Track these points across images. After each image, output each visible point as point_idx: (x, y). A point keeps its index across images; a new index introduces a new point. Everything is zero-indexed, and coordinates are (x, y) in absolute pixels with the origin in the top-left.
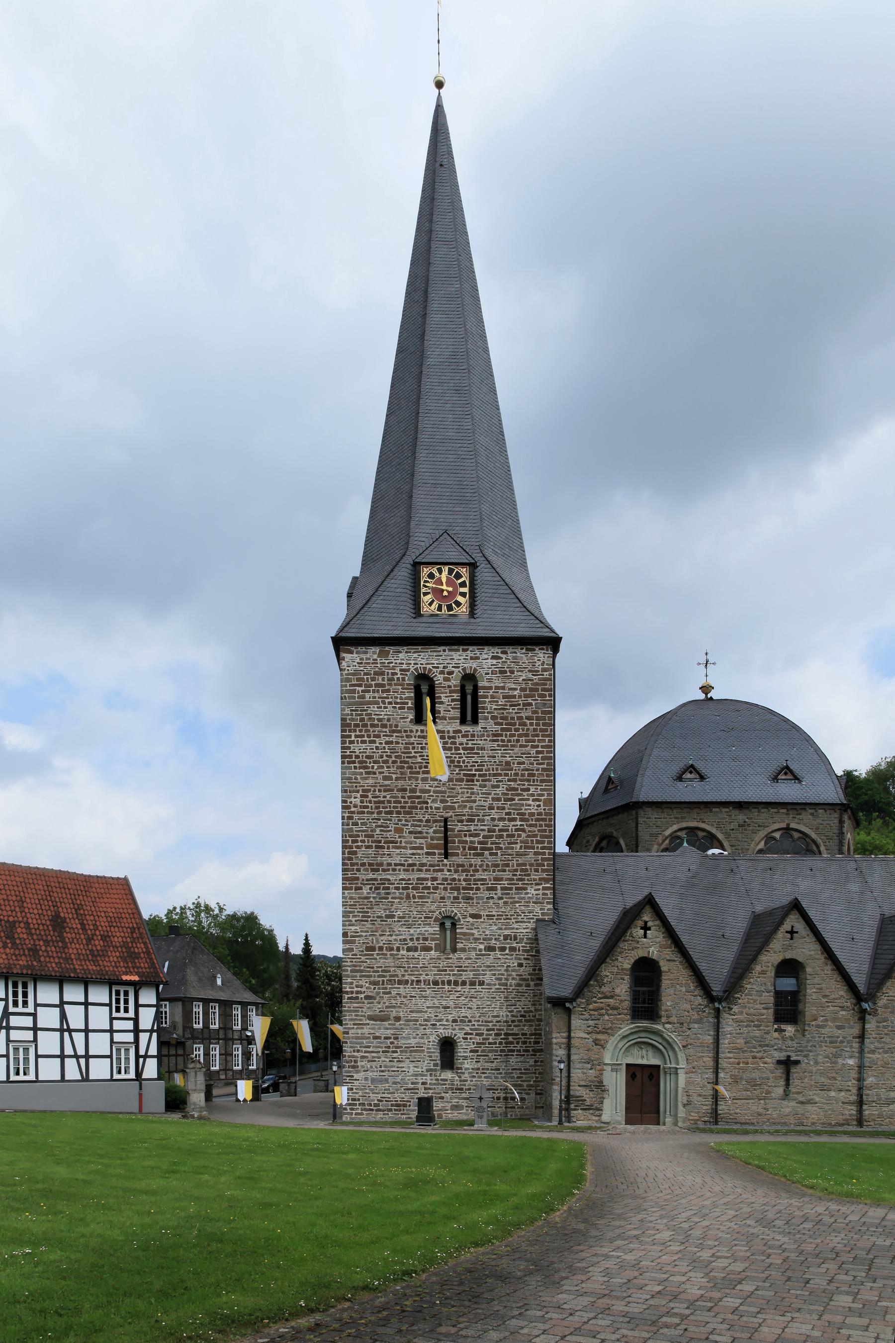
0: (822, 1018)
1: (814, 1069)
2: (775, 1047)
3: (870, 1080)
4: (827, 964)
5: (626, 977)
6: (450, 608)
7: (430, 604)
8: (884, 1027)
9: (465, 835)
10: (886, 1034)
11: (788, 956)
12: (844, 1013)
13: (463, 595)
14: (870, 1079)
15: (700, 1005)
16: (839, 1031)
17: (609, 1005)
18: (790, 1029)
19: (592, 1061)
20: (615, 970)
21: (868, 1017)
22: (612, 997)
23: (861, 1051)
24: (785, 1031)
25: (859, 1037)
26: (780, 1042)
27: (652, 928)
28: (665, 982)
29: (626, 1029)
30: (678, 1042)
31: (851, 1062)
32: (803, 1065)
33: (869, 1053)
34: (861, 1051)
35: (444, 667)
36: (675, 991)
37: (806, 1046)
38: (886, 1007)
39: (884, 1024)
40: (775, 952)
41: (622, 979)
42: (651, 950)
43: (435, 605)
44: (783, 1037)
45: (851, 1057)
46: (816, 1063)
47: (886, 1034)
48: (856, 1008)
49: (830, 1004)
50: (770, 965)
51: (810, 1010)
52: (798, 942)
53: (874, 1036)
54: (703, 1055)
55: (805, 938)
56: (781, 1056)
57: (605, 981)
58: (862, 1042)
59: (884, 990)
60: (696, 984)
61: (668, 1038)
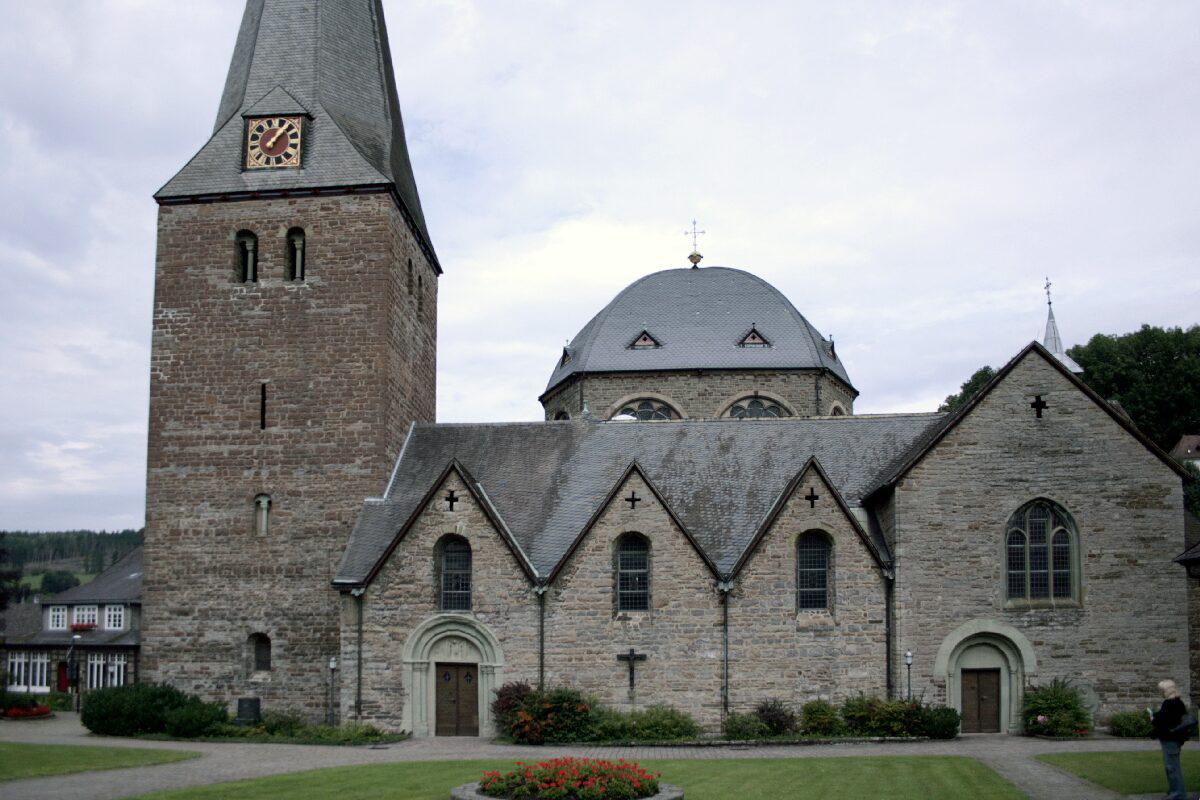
0: (674, 603)
1: (666, 665)
2: (616, 640)
3: (737, 676)
4: (678, 537)
5: (429, 558)
6: (279, 160)
7: (258, 158)
8: (753, 611)
9: (285, 403)
10: (755, 620)
11: (629, 528)
12: (701, 595)
13: (294, 146)
14: (737, 676)
15: (519, 589)
16: (696, 618)
17: (408, 592)
18: (637, 617)
19: (389, 659)
20: (415, 549)
21: (731, 600)
22: (411, 582)
23: (726, 642)
24: (630, 619)
25: (721, 625)
26: (621, 633)
27: (460, 499)
28: (476, 563)
29: (432, 618)
30: (494, 636)
31: (712, 655)
32: (652, 661)
33: (734, 643)
34: (726, 642)
35: (269, 222)
36: (488, 573)
37: (655, 638)
38: (753, 586)
39: (753, 607)
40: (613, 524)
41: (423, 559)
42: (459, 525)
43: (263, 159)
44: (625, 627)
45: (712, 649)
46: (668, 657)
47: (755, 620)
48: (715, 589)
49: (683, 585)
50: (607, 539)
51: (657, 593)
52: (640, 511)
53: (740, 622)
54: (524, 650)
55: (648, 506)
56: (624, 650)
57: (403, 563)
58: (726, 630)
59: (751, 566)
60: (514, 565)
61: (480, 629)
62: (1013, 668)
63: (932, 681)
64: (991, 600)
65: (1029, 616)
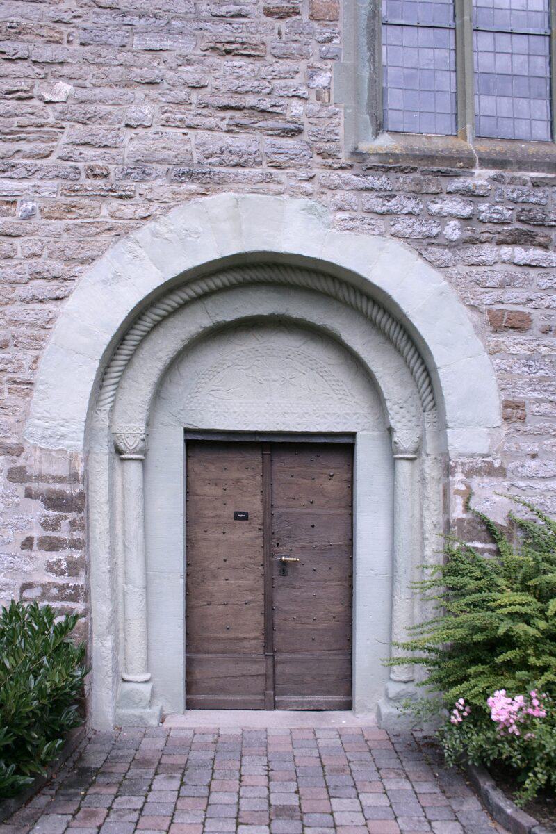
62: (405, 438)
63: (17, 475)
64: (296, 109)
65: (470, 195)
